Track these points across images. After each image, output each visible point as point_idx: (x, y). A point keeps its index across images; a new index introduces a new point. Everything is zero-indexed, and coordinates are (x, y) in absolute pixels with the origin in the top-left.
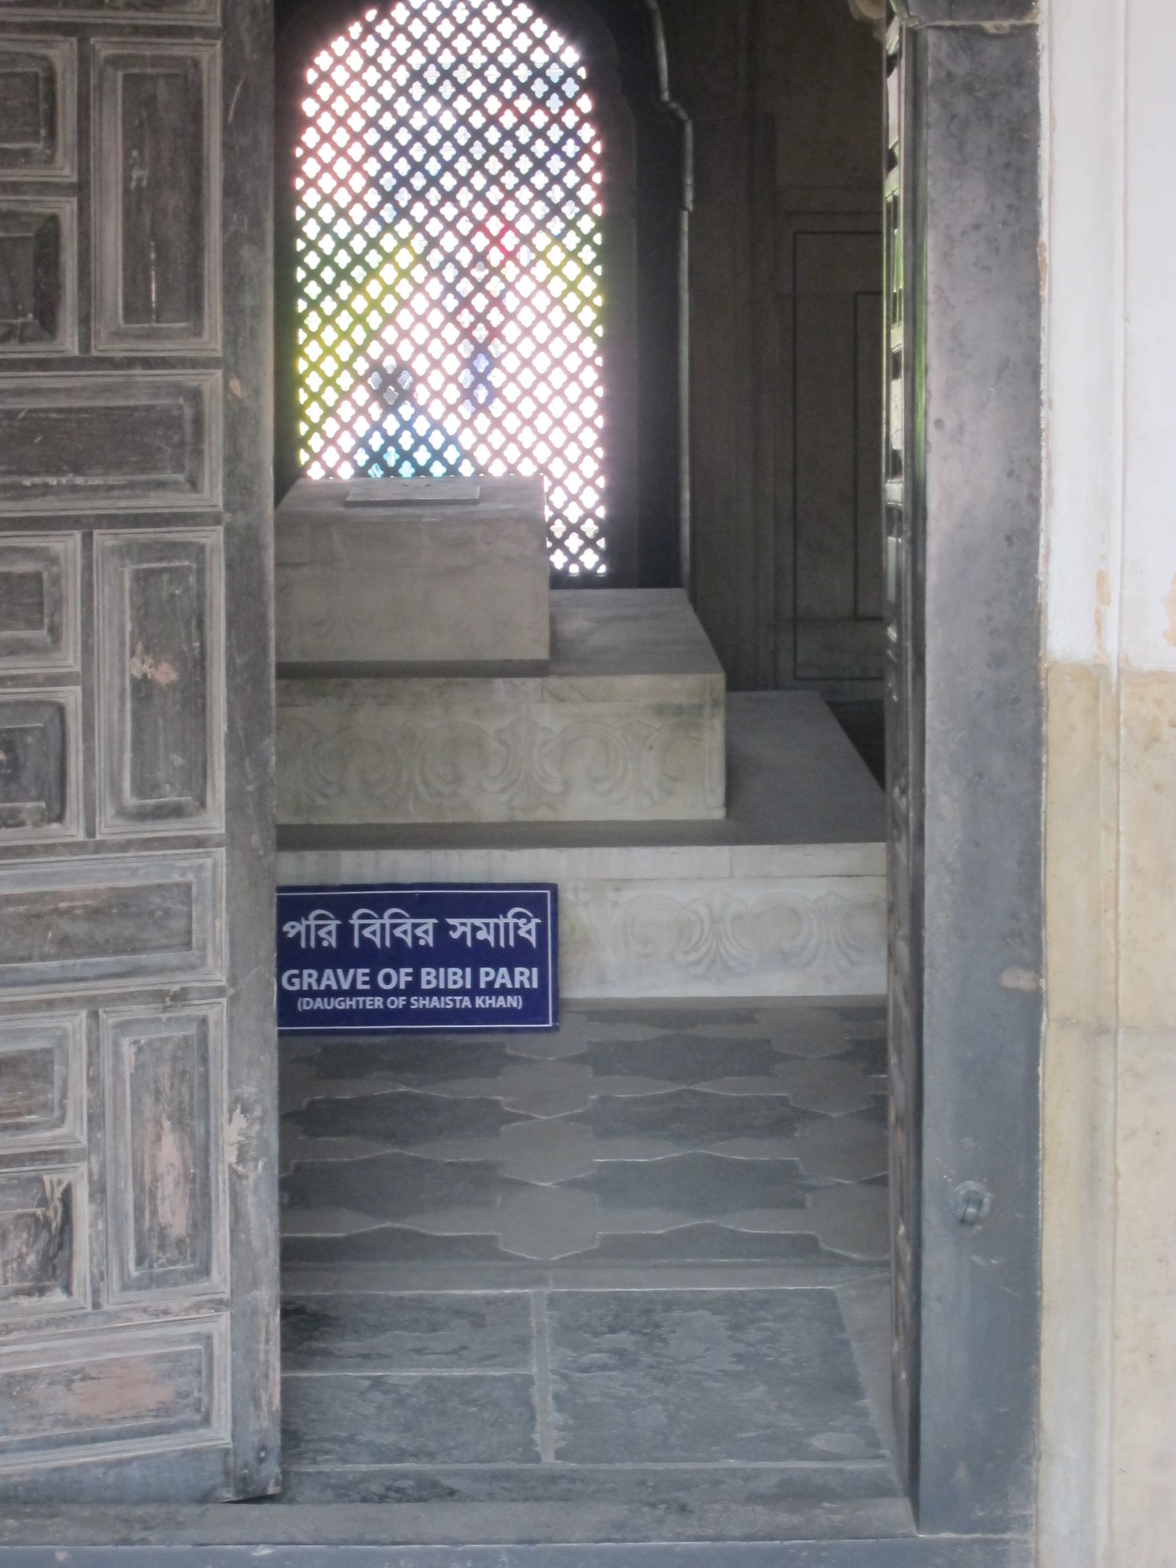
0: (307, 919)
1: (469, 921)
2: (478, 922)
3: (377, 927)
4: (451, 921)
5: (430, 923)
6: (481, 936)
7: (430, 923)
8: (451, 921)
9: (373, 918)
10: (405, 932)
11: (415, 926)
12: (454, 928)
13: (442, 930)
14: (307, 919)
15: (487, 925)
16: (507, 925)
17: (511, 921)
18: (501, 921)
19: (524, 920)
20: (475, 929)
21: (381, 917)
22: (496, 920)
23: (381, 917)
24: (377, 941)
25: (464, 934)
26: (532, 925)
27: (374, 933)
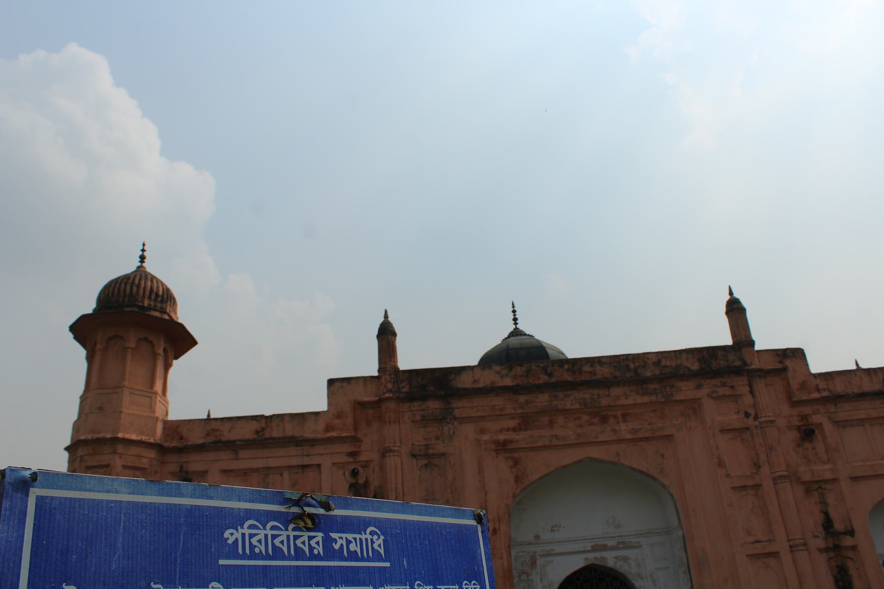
0: (242, 528)
1: (344, 535)
2: (350, 536)
3: (284, 538)
4: (334, 535)
5: (320, 536)
6: (353, 547)
7: (320, 536)
8: (334, 535)
9: (281, 530)
10: (303, 543)
11: (310, 538)
12: (335, 541)
13: (328, 542)
14: (242, 528)
15: (355, 539)
16: (366, 539)
17: (369, 537)
18: (363, 537)
19: (375, 537)
20: (349, 542)
21: (287, 530)
22: (359, 536)
23: (287, 530)
24: (285, 549)
25: (342, 545)
26: (381, 541)
27: (282, 542)
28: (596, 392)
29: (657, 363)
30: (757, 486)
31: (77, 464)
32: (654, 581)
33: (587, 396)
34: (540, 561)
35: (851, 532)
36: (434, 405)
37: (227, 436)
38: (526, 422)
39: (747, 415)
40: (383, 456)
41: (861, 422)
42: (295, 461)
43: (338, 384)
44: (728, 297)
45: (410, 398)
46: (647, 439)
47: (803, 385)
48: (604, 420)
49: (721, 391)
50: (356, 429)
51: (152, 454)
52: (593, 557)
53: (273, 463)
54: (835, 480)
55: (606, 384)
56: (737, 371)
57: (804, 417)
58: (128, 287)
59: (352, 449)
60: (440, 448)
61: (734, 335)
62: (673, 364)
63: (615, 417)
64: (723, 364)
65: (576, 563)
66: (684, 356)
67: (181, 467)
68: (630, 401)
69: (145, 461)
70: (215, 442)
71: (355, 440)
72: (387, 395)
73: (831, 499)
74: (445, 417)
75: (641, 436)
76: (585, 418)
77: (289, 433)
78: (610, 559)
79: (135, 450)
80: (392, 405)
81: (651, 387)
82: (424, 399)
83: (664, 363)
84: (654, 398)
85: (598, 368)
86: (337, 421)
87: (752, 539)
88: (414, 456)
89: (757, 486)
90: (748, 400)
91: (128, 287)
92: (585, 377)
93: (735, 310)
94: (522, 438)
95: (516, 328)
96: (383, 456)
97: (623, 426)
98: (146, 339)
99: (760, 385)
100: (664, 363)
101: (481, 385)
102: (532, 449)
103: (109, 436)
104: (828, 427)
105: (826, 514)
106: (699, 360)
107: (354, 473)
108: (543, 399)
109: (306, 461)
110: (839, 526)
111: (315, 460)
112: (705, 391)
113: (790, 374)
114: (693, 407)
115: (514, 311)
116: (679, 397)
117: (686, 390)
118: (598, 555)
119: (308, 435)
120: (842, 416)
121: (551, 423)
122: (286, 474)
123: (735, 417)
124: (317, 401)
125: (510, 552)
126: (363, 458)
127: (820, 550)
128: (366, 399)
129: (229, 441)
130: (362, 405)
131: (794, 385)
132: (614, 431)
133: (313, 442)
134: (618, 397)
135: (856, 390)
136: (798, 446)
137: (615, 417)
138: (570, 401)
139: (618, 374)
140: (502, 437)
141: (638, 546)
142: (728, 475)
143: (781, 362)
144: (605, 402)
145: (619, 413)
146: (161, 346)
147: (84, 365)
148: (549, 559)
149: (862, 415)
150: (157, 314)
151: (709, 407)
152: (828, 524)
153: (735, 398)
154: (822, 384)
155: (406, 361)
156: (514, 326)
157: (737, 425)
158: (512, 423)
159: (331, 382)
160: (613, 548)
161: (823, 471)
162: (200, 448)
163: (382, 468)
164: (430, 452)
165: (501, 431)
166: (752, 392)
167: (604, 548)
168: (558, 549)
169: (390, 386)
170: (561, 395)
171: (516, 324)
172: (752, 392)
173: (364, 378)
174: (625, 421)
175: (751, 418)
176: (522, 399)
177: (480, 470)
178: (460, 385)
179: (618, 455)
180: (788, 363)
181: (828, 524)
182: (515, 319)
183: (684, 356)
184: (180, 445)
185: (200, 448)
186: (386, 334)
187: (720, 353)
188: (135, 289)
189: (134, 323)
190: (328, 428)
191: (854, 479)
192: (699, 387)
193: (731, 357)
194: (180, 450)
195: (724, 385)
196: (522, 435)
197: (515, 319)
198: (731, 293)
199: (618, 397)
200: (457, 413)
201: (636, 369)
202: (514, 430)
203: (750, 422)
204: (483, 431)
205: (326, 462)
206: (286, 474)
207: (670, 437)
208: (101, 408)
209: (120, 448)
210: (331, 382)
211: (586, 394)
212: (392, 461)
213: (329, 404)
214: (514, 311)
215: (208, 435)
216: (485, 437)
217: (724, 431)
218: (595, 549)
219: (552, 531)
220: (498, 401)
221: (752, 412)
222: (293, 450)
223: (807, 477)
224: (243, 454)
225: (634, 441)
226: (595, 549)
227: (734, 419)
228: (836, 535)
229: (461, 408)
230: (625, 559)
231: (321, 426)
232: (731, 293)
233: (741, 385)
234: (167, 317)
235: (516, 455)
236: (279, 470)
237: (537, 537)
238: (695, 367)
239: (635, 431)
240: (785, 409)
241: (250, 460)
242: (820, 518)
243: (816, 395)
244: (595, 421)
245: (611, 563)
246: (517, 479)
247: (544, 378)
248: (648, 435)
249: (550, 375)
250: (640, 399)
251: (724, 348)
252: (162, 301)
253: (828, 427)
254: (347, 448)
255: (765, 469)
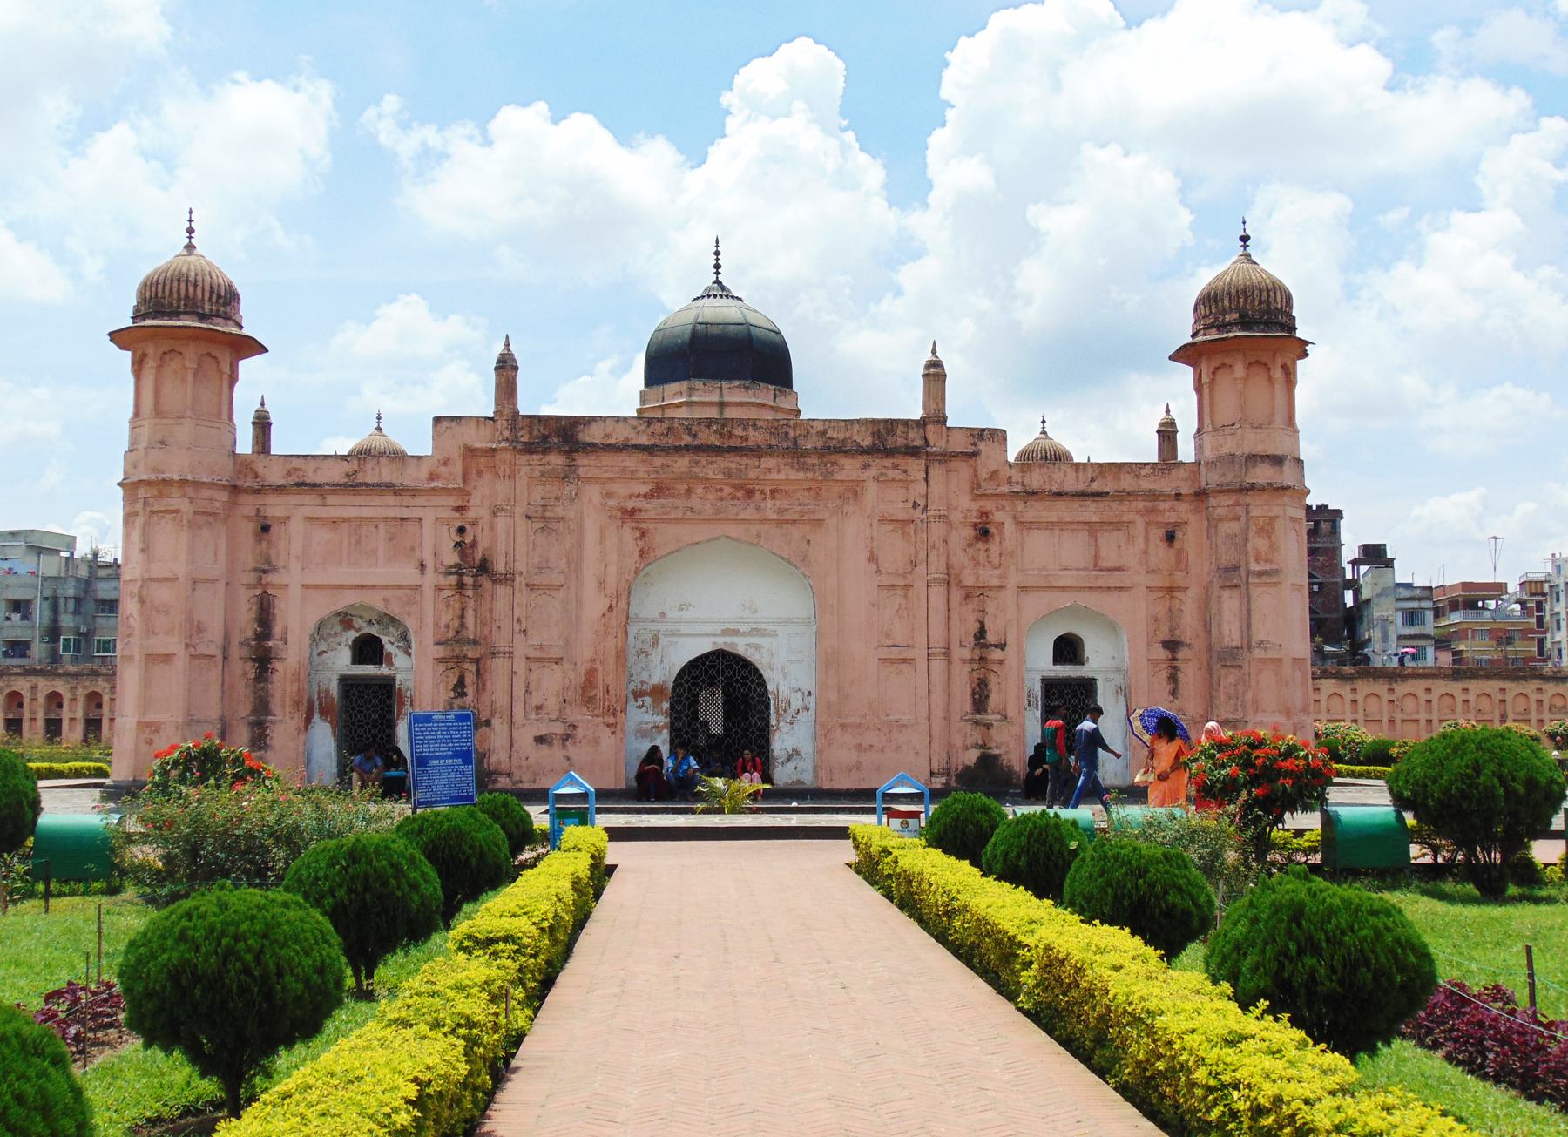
28: (744, 461)
29: (823, 433)
30: (907, 587)
31: (139, 506)
32: (785, 675)
33: (733, 465)
34: (663, 641)
35: (1002, 646)
36: (556, 460)
37: (311, 478)
38: (659, 491)
39: (915, 505)
40: (494, 514)
41: (1050, 526)
42: (391, 513)
43: (445, 424)
44: (929, 356)
45: (529, 449)
46: (795, 521)
47: (993, 475)
48: (750, 493)
49: (892, 474)
50: (465, 480)
51: (224, 496)
52: (721, 643)
53: (367, 512)
54: (1001, 587)
55: (756, 452)
56: (913, 452)
57: (984, 513)
58: (183, 286)
59: (459, 503)
60: (559, 511)
61: (924, 408)
62: (842, 436)
63: (762, 492)
64: (900, 441)
65: (705, 647)
66: (856, 427)
67: (258, 511)
68: (782, 476)
69: (217, 504)
70: (299, 485)
71: (463, 492)
72: (503, 444)
73: (990, 609)
74: (568, 475)
75: (787, 517)
76: (727, 490)
77: (386, 479)
78: (741, 647)
79: (206, 493)
80: (507, 456)
81: (809, 461)
82: (545, 452)
83: (829, 434)
84: (810, 475)
85: (751, 432)
86: (443, 468)
87: (890, 643)
88: (528, 517)
89: (907, 587)
90: (921, 487)
91: (183, 286)
92: (736, 442)
93: (935, 374)
94: (652, 507)
95: (717, 282)
96: (494, 514)
97: (769, 503)
98: (209, 354)
99: (936, 472)
100: (829, 434)
101: (612, 441)
102: (663, 521)
103: (177, 478)
104: (1009, 528)
105: (982, 624)
106: (873, 434)
107: (461, 530)
108: (682, 463)
109: (406, 513)
110: (991, 638)
111: (417, 513)
112: (872, 472)
113: (982, 459)
114: (854, 491)
115: (717, 253)
116: (837, 476)
117: (850, 468)
118: (728, 639)
119: (408, 481)
120: (1029, 516)
121: (689, 491)
122: (381, 525)
123: (901, 505)
124: (418, 442)
125: (626, 632)
126: (471, 514)
127: (964, 661)
128: (478, 445)
129: (315, 485)
130: (470, 452)
131: (983, 475)
132: (758, 508)
133: (414, 492)
134: (769, 470)
135: (1055, 489)
136: (970, 545)
137: (762, 492)
138: (713, 469)
139: (774, 442)
140: (630, 505)
141: (774, 635)
142: (878, 571)
143: (974, 444)
144: (752, 474)
145: (768, 489)
146: (225, 358)
147: (131, 379)
148: (674, 639)
149: (1053, 517)
150: (221, 327)
151: (872, 489)
152: (981, 633)
153: (906, 484)
154: (1016, 476)
155: (528, 404)
156: (714, 277)
157: (901, 516)
158: (644, 489)
159: (437, 420)
160: (744, 634)
161: (990, 577)
162: (280, 489)
163: (492, 527)
164: (548, 514)
165: (630, 497)
166: (927, 480)
167: (736, 632)
168: (684, 629)
169: (507, 433)
170: (703, 461)
171: (717, 273)
172: (927, 480)
173: (478, 420)
174: (773, 498)
175: (919, 510)
176: (658, 461)
177: (602, 540)
178: (588, 440)
179: (759, 536)
180: (982, 446)
181: (981, 633)
182: (717, 266)
183: (856, 427)
184: (256, 486)
185: (280, 489)
186: (506, 367)
187: (901, 428)
188: (191, 289)
189: (187, 326)
190: (432, 477)
191: (1023, 589)
192: (865, 467)
193: (911, 435)
194: (257, 491)
195: (895, 467)
196: (655, 502)
197: (717, 266)
198: (934, 352)
199: (769, 470)
200: (581, 471)
201: (795, 438)
202: (645, 496)
203: (917, 513)
204: (609, 495)
205: (429, 516)
206: (381, 525)
207: (820, 522)
208: (162, 442)
209: (190, 491)
210: (437, 420)
211: (732, 462)
212: (502, 522)
213: (435, 447)
214: (717, 253)
215: (289, 474)
216: (612, 503)
217: (882, 520)
218: (725, 633)
219: (681, 609)
220: (629, 461)
221: (922, 503)
222: (390, 499)
223: (969, 581)
224: (331, 500)
225: (780, 523)
226: (725, 633)
227: (899, 510)
228: (986, 646)
229: (585, 463)
230: (757, 647)
231: (424, 475)
232: (934, 352)
233: (915, 466)
234: (235, 330)
235: (644, 526)
236: (373, 522)
237: (663, 614)
238: (867, 442)
239: (782, 511)
240: (965, 502)
241: (341, 507)
242: (973, 627)
243: (1005, 489)
244: (739, 495)
245: (741, 650)
246: (642, 553)
247: (686, 439)
248: (796, 517)
249: (695, 436)
250: (793, 475)
251: (905, 423)
252: (226, 304)
253: (1009, 528)
254: (454, 501)
255: (921, 569)
